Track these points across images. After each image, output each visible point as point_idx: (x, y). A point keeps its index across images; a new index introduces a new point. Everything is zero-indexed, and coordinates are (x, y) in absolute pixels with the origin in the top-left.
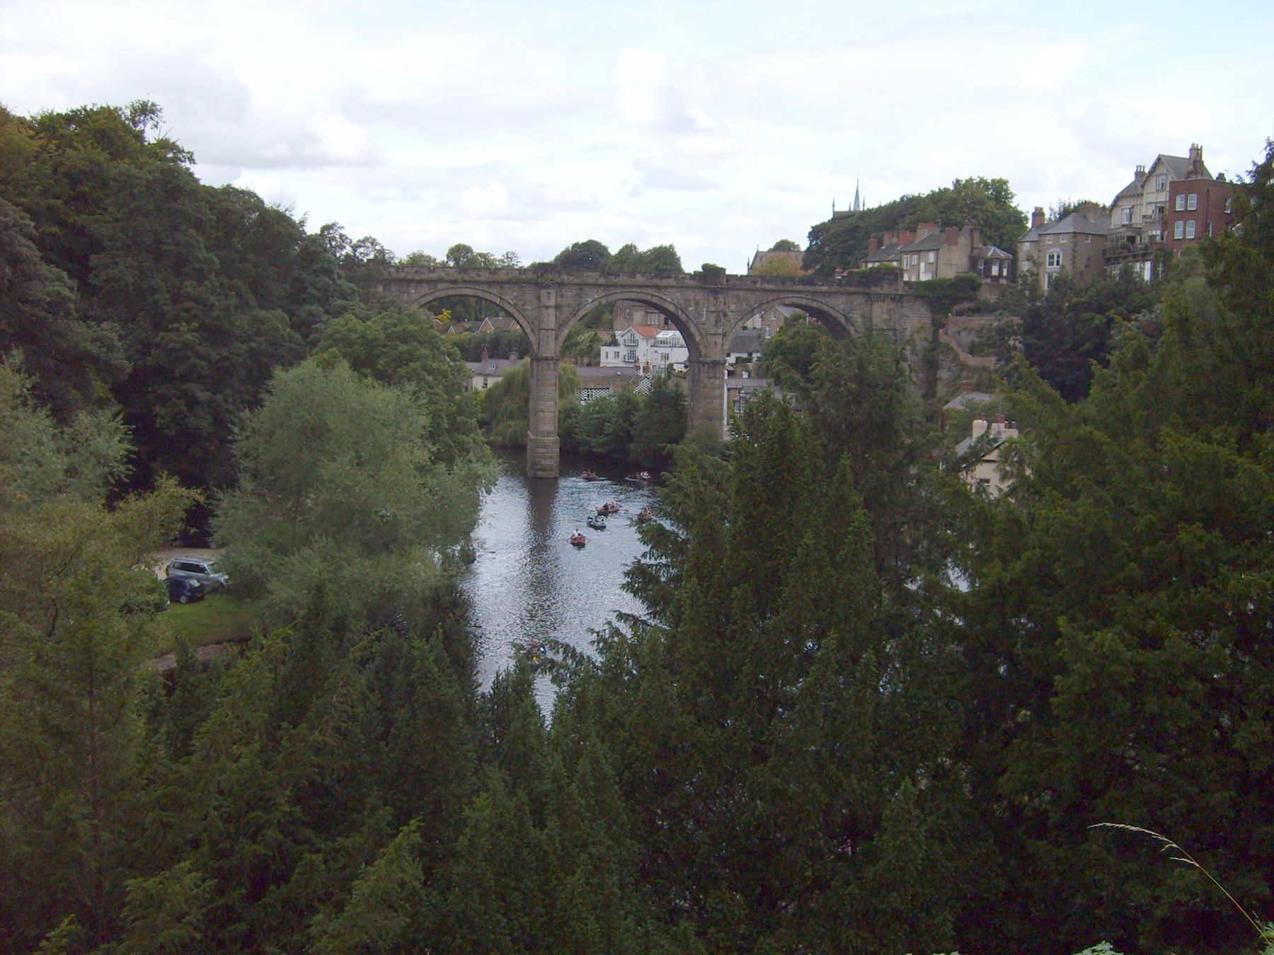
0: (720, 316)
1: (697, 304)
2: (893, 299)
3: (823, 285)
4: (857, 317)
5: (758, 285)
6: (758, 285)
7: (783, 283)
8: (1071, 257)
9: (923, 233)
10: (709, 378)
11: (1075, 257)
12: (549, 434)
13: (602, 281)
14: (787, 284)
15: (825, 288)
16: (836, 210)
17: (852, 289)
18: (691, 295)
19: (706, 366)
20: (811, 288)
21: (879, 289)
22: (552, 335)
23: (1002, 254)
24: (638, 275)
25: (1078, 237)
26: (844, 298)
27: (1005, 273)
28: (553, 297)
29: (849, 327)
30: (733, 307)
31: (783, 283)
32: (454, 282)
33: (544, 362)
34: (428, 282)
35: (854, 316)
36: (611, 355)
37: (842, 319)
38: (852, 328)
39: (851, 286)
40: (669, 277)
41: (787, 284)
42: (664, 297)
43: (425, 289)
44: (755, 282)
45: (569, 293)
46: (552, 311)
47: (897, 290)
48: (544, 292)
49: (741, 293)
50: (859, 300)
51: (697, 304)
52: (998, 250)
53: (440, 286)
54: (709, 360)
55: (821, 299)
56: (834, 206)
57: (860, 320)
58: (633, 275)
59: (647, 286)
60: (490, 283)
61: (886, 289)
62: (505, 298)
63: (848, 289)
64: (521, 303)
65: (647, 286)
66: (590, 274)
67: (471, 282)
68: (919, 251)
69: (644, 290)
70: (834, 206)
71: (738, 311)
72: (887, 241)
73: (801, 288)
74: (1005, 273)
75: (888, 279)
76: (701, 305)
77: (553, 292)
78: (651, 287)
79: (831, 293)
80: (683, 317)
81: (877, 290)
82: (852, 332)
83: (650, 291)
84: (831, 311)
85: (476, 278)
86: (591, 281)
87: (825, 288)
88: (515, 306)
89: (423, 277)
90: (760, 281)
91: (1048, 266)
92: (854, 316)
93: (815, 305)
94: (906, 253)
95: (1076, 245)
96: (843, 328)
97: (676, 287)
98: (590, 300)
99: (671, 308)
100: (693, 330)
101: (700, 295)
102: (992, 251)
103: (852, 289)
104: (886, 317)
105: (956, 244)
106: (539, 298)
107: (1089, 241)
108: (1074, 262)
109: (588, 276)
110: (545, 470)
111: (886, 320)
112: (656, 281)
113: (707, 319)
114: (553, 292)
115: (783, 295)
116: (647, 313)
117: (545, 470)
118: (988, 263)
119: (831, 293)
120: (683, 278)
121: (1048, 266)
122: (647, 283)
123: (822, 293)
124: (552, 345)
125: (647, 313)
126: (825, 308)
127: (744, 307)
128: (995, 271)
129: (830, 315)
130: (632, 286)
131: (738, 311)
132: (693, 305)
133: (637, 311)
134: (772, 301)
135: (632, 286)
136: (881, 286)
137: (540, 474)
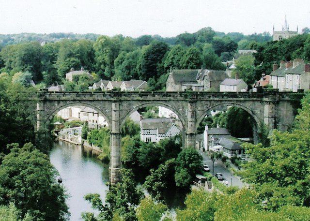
0: (194, 114)
1: (183, 108)
2: (274, 103)
3: (241, 97)
4: (258, 112)
5: (211, 98)
6: (211, 98)
7: (223, 97)
15: (242, 99)
16: (275, 30)
17: (255, 99)
18: (180, 103)
19: (188, 136)
20: (235, 99)
21: (267, 99)
24: (156, 96)
28: (118, 106)
29: (254, 116)
30: (199, 108)
31: (223, 97)
32: (74, 100)
34: (63, 101)
35: (256, 111)
37: (250, 113)
40: (170, 96)
44: (210, 97)
45: (125, 104)
46: (117, 112)
48: (113, 104)
49: (203, 102)
50: (258, 104)
51: (183, 108)
53: (68, 102)
57: (259, 112)
58: (154, 95)
64: (104, 109)
66: (134, 95)
67: (81, 100)
73: (231, 99)
78: (162, 101)
79: (245, 101)
82: (256, 118)
84: (245, 109)
85: (84, 99)
87: (242, 99)
98: (135, 107)
101: (184, 104)
114: (118, 104)
115: (223, 102)
116: (182, 85)
119: (245, 101)
123: (241, 101)
125: (182, 85)
126: (243, 107)
127: (205, 108)
130: (153, 101)
132: (181, 107)
133: (176, 84)
135: (153, 101)
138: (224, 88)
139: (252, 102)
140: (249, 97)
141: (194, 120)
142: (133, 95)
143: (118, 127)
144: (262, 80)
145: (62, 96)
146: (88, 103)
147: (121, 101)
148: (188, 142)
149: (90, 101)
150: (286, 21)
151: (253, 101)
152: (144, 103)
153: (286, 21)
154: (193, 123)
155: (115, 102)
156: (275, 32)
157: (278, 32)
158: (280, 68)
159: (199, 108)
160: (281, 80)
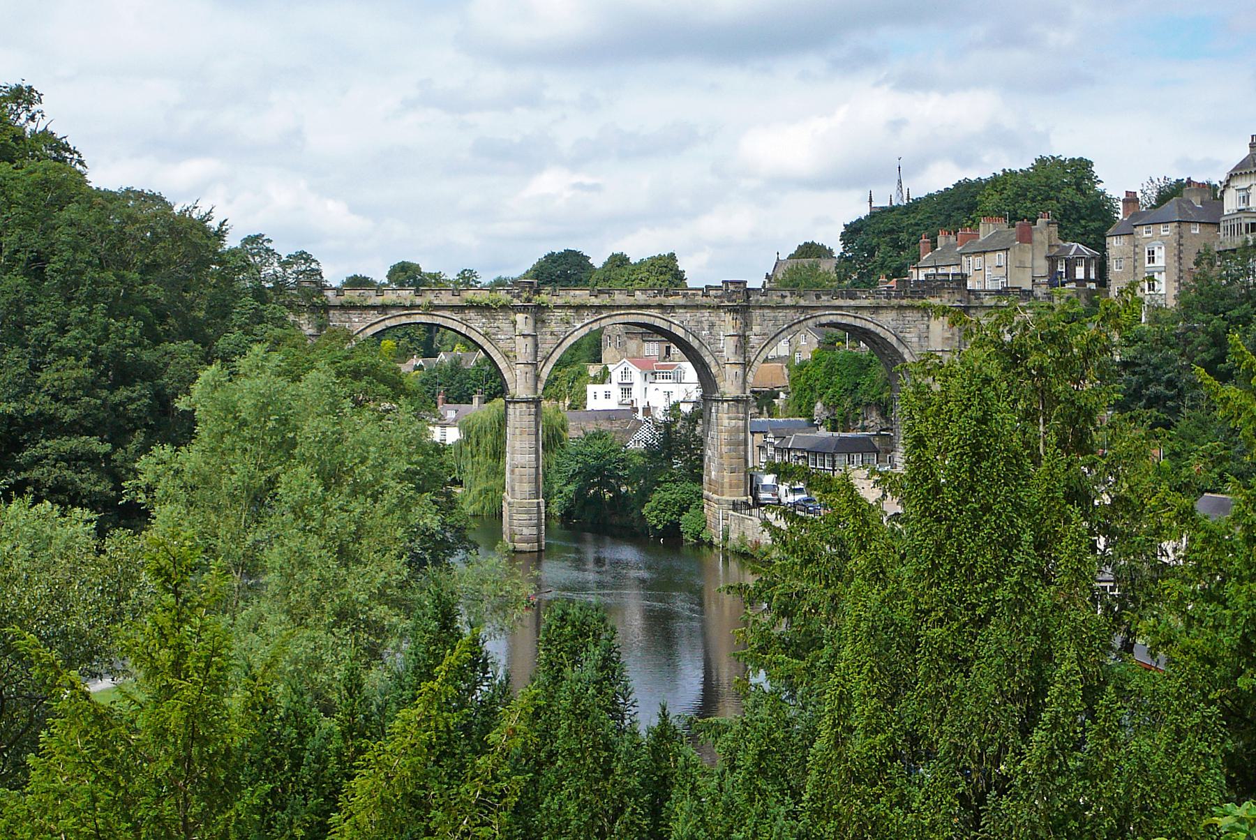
1: (712, 325)
3: (866, 298)
4: (912, 337)
7: (818, 297)
8: (1177, 253)
9: (986, 230)
10: (730, 418)
11: (1180, 252)
14: (824, 298)
17: (905, 302)
20: (852, 303)
23: (1087, 252)
25: (1184, 226)
27: (1093, 276)
28: (531, 322)
29: (901, 349)
31: (818, 297)
35: (907, 335)
36: (601, 395)
38: (907, 351)
39: (903, 298)
40: (677, 294)
41: (824, 298)
42: (670, 319)
43: (373, 316)
44: (783, 297)
47: (960, 301)
48: (520, 317)
51: (712, 325)
52: (1080, 246)
54: (728, 396)
55: (866, 315)
56: (871, 201)
59: (648, 307)
62: (472, 325)
65: (648, 307)
66: (577, 292)
68: (984, 252)
70: (871, 201)
71: (764, 334)
72: (941, 240)
74: (1093, 276)
75: (947, 289)
76: (716, 328)
80: (695, 344)
81: (935, 301)
84: (879, 330)
85: (436, 302)
86: (577, 301)
88: (486, 335)
89: (370, 302)
90: (788, 294)
91: (1147, 265)
92: (907, 335)
93: (858, 323)
94: (968, 255)
95: (1181, 237)
96: (895, 351)
97: (685, 307)
99: (680, 332)
100: (708, 359)
102: (1075, 247)
103: (905, 302)
104: (948, 335)
105: (1030, 241)
106: (514, 323)
107: (1198, 232)
108: (1180, 258)
109: (574, 296)
111: (948, 339)
112: (660, 299)
113: (728, 347)
118: (1071, 265)
119: (876, 309)
120: (694, 294)
121: (1147, 265)
122: (649, 302)
126: (871, 326)
128: (1080, 273)
129: (877, 335)
131: (764, 334)
132: (706, 327)
133: (631, 339)
134: (805, 319)
136: (940, 297)
139: (894, 313)
140: (888, 297)
142: (572, 293)
143: (531, 382)
145: (373, 293)
146: (447, 314)
147: (541, 308)
148: (726, 422)
151: (901, 307)
154: (739, 370)
155: (523, 309)
158: (939, 249)
159: (756, 329)
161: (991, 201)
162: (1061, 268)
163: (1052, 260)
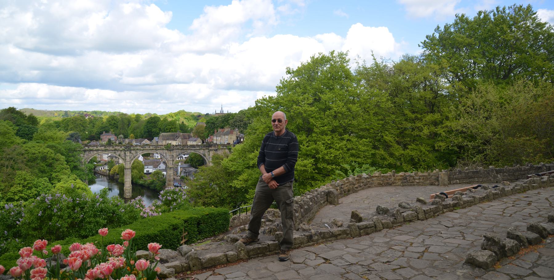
12: (129, 187)
13: (142, 149)
15: (198, 148)
17: (205, 148)
20: (194, 148)
22: (129, 162)
24: (151, 147)
26: (203, 150)
29: (204, 157)
30: (175, 154)
31: (187, 147)
33: (127, 170)
37: (203, 156)
48: (126, 152)
50: (207, 150)
55: (198, 151)
59: (153, 150)
60: (112, 150)
61: (213, 148)
63: (204, 148)
69: (152, 151)
73: (192, 148)
77: (129, 152)
81: (210, 148)
82: (205, 158)
83: (153, 151)
87: (198, 148)
101: (166, 151)
106: (125, 154)
110: (127, 196)
117: (127, 196)
124: (129, 165)
126: (198, 153)
128: (242, 140)
132: (165, 153)
137: (126, 197)
138: (189, 143)
141: (172, 160)
144: (209, 138)
146: (111, 151)
149: (112, 150)
150: (222, 108)
152: (145, 151)
153: (222, 108)
156: (216, 113)
157: (218, 114)
160: (219, 139)
161: (231, 121)
162: (239, 139)
163: (237, 137)
